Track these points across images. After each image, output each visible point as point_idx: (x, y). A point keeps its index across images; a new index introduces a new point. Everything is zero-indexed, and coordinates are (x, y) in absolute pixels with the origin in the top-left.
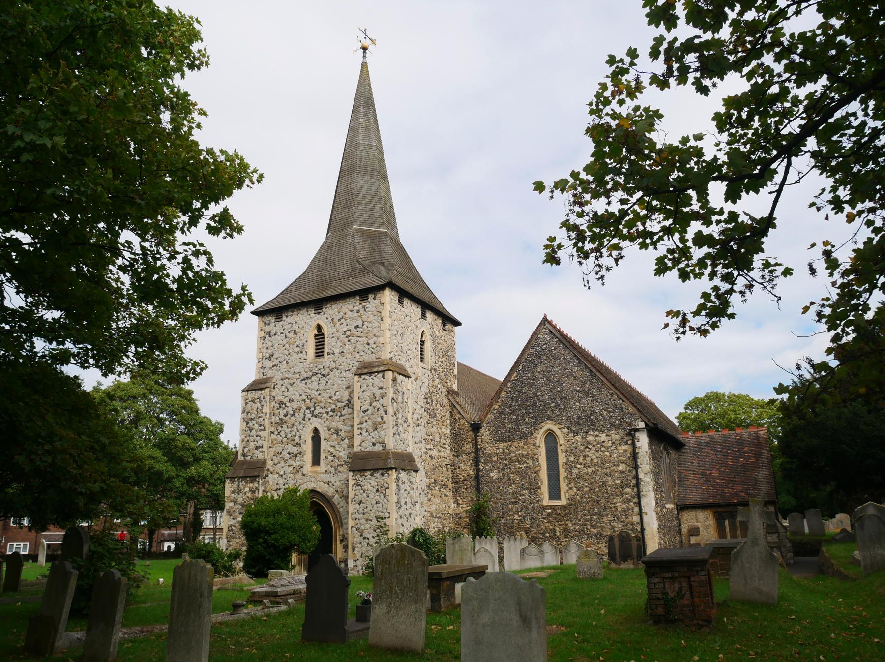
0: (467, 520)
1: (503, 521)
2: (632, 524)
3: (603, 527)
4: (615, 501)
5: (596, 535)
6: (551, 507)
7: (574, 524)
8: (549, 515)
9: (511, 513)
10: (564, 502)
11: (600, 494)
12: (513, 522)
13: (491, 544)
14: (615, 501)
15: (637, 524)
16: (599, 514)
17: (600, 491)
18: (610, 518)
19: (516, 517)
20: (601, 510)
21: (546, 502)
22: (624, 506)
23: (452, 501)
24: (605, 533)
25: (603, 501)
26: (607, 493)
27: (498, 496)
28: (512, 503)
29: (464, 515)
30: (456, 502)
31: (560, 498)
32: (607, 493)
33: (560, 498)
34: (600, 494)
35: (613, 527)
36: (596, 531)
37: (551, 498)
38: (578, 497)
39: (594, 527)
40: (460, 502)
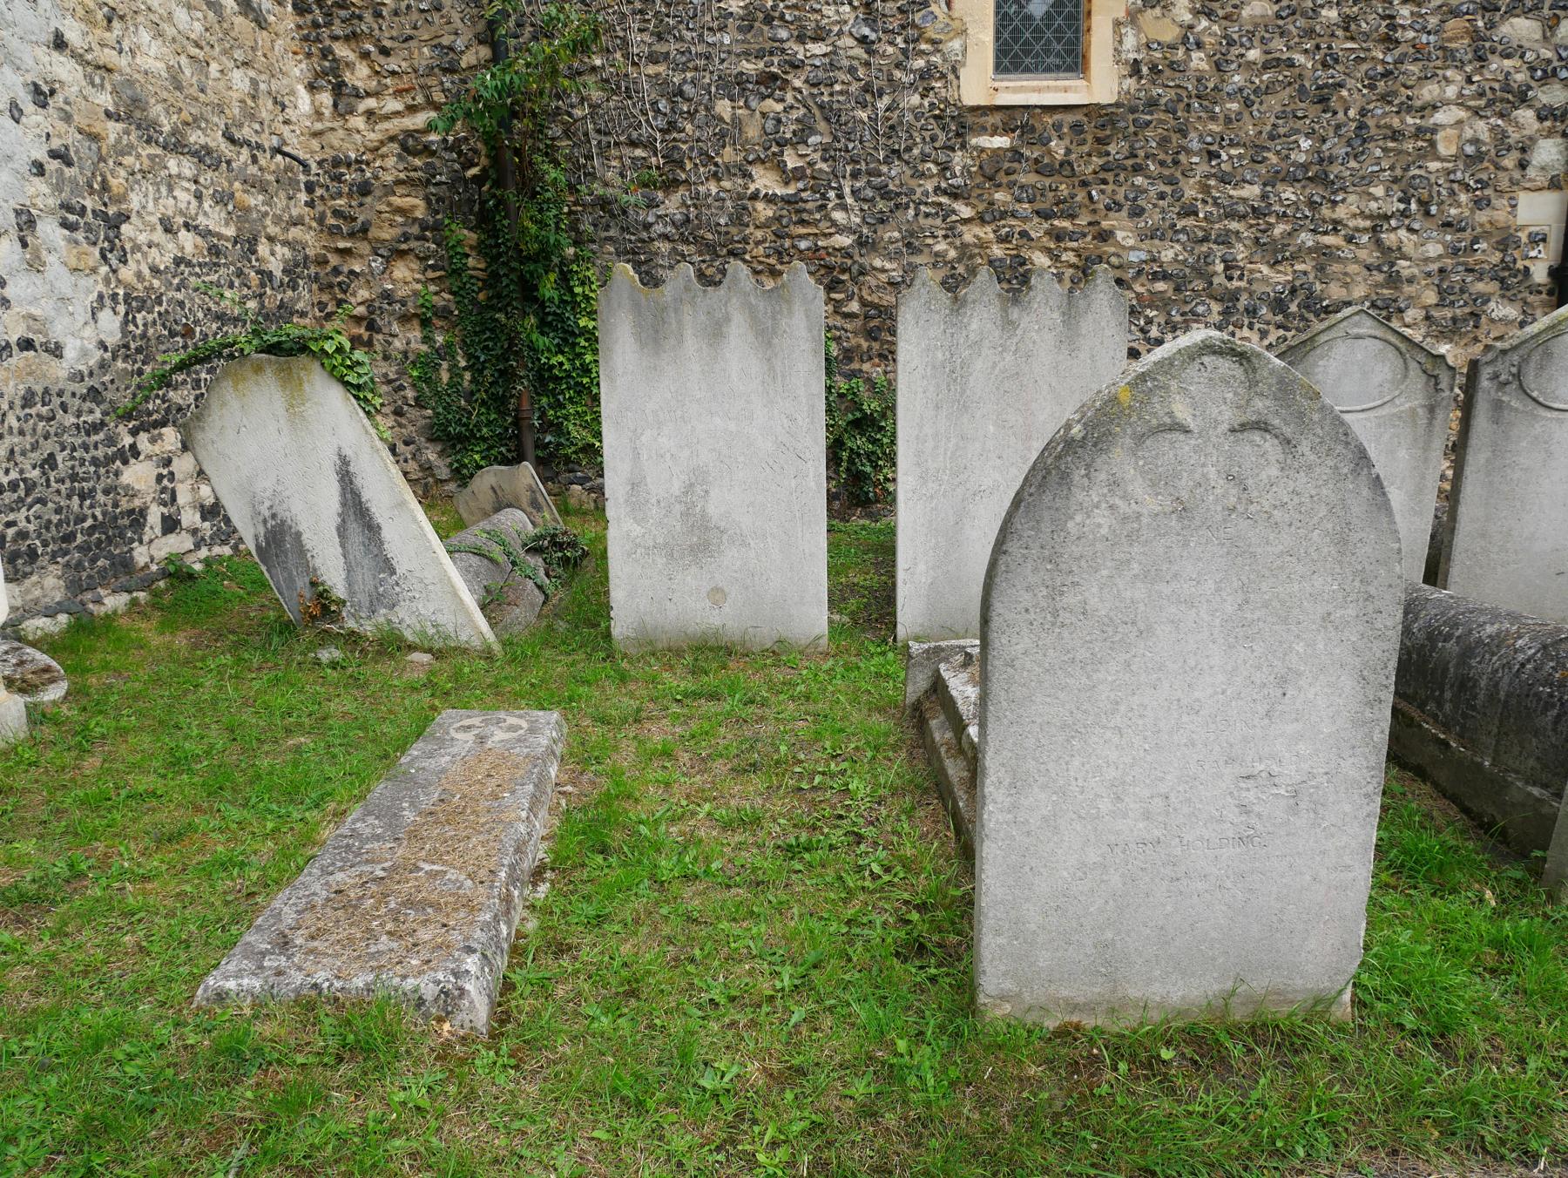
0: (416, 203)
1: (672, 205)
2: (1506, 241)
3: (1325, 255)
4: (1429, 92)
5: (1279, 305)
6: (1012, 118)
7: (1152, 234)
8: (992, 170)
9: (728, 155)
10: (1102, 83)
11: (1342, 45)
12: (740, 217)
13: (766, 335)
14: (1429, 92)
15: (1538, 239)
16: (1319, 175)
17: (1347, 22)
18: (1381, 197)
19: (765, 181)
20: (1335, 147)
21: (978, 82)
22: (1481, 128)
23: (298, 70)
24: (1336, 292)
25: (1353, 96)
26: (1389, 41)
27: (639, 41)
28: (737, 86)
29: (390, 167)
30: (329, 77)
31: (1074, 61)
32: (1389, 41)
33: (1074, 61)
34: (1342, 45)
35: (1390, 255)
36: (1277, 278)
37: (1013, 54)
38: (1199, 61)
39: (1277, 254)
40: (359, 76)
